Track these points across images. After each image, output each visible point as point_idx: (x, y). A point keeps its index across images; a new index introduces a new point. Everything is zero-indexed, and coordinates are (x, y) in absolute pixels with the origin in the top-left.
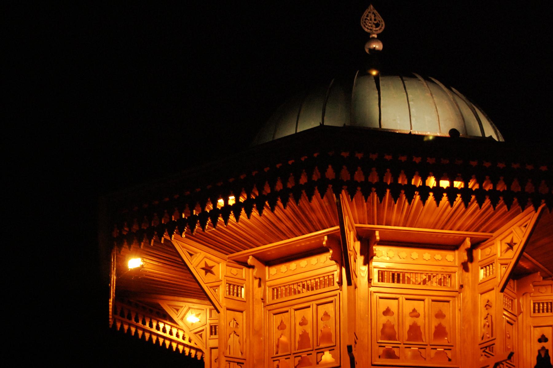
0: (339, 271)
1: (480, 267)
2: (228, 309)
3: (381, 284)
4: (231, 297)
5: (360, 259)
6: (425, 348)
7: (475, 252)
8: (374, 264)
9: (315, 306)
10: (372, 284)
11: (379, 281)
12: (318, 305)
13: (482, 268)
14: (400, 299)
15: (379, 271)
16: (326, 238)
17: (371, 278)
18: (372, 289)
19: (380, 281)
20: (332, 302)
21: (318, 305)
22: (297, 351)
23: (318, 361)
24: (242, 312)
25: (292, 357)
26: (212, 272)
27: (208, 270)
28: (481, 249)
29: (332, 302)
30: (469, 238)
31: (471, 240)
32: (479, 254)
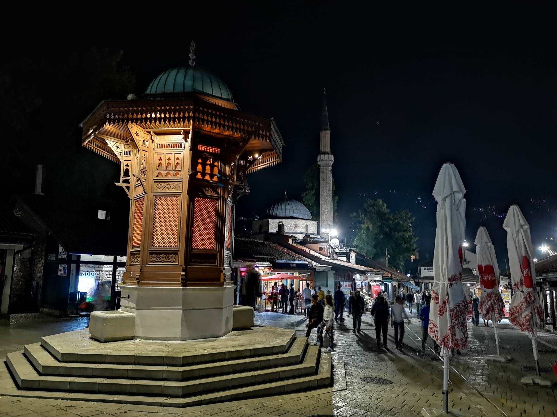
0: (184, 143)
2: (143, 150)
4: (143, 145)
24: (147, 152)
26: (138, 135)
27: (137, 134)
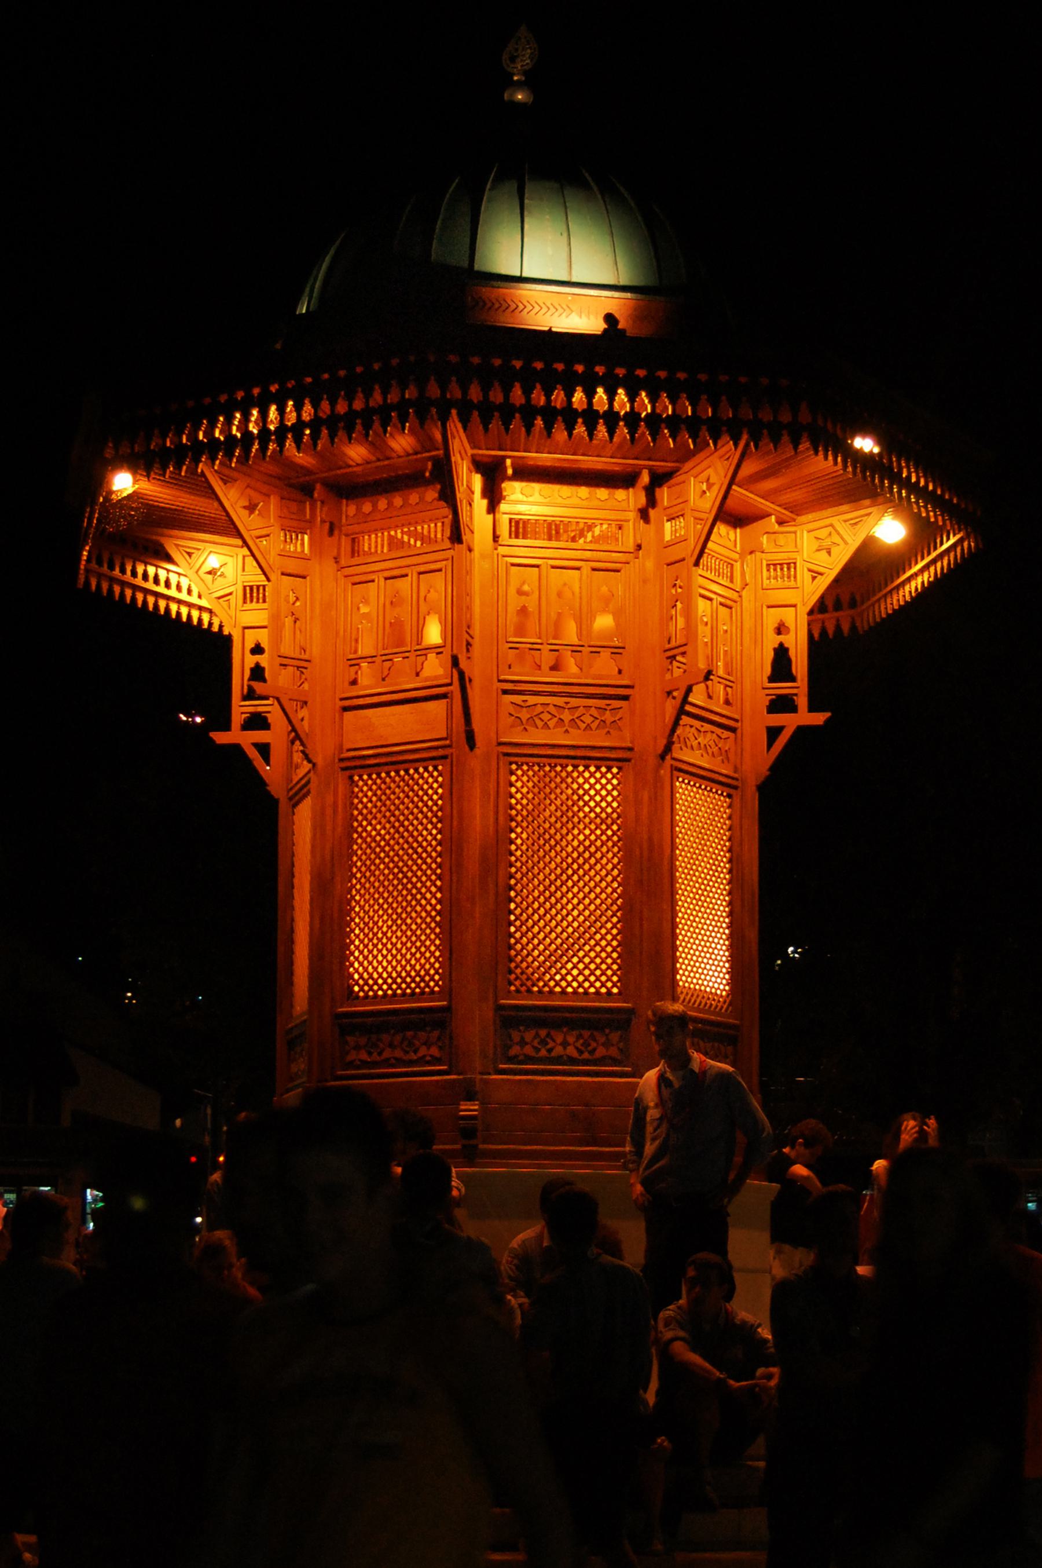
1: (665, 518)
3: (515, 541)
5: (485, 502)
6: (580, 652)
7: (658, 491)
8: (503, 507)
9: (415, 575)
10: (500, 542)
11: (510, 537)
12: (420, 573)
13: (668, 520)
14: (544, 569)
15: (511, 520)
16: (430, 465)
17: (498, 533)
18: (502, 550)
19: (513, 536)
20: (440, 570)
21: (420, 573)
22: (386, 652)
23: (418, 670)
25: (378, 660)
28: (669, 487)
29: (440, 570)
30: (647, 471)
31: (650, 472)
32: (664, 495)
